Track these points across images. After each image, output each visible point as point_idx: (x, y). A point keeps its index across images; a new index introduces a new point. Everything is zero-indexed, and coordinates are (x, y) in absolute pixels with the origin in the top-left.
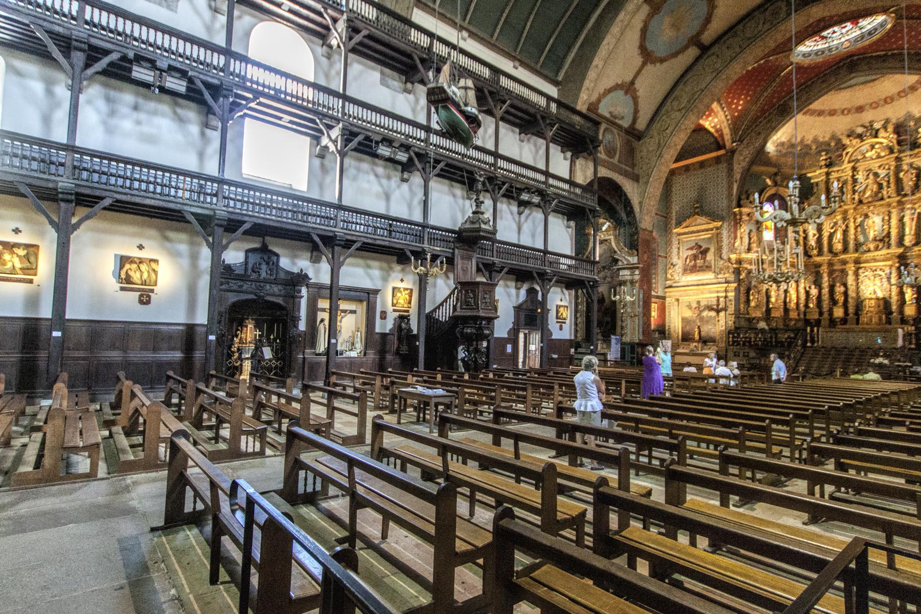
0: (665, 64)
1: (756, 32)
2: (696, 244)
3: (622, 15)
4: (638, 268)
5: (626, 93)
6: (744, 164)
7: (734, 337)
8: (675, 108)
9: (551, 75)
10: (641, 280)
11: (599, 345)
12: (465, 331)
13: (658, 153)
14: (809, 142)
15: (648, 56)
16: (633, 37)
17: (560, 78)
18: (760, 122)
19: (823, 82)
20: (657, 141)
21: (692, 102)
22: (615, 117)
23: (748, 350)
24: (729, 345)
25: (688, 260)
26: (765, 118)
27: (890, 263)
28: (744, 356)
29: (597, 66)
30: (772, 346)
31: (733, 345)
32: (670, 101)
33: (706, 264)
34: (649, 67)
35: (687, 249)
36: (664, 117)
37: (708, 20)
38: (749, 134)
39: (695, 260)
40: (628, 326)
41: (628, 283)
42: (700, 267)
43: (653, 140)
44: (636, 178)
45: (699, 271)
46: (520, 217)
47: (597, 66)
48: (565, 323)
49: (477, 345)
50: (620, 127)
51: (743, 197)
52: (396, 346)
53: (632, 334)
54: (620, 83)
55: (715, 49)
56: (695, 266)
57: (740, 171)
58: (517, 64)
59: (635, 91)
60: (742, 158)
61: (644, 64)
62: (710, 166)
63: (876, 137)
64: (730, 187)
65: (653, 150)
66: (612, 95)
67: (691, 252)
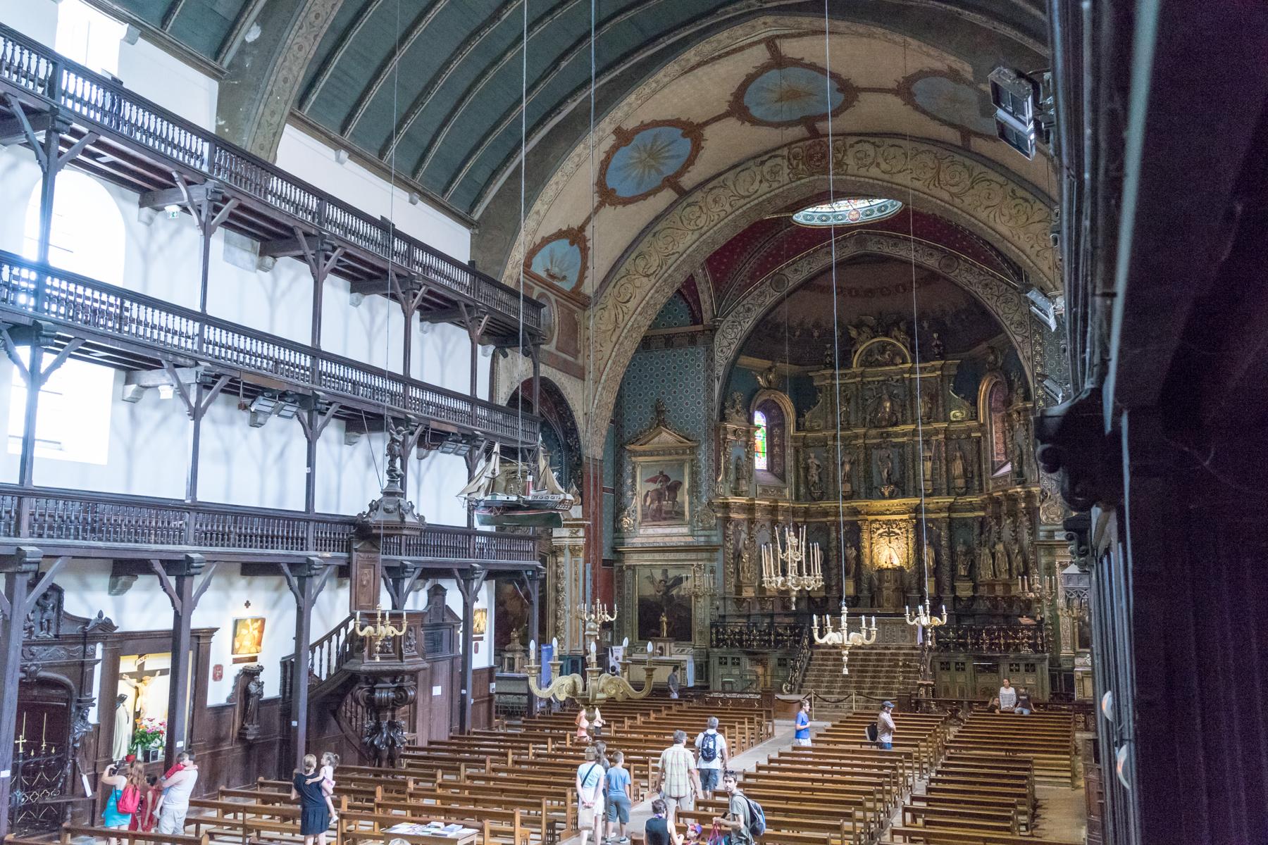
0: (632, 208)
1: (751, 190)
2: (661, 473)
3: (580, 149)
4: (583, 526)
5: (572, 244)
6: (730, 353)
7: (717, 632)
8: (641, 270)
9: (462, 212)
10: (588, 545)
11: (517, 660)
12: (377, 695)
13: (614, 339)
14: (810, 326)
15: (606, 195)
16: (590, 172)
17: (477, 216)
18: (750, 293)
20: (613, 316)
21: (665, 268)
22: (552, 277)
24: (712, 647)
25: (649, 500)
26: (756, 289)
27: (905, 517)
28: (733, 664)
29: (538, 213)
31: (717, 646)
32: (633, 256)
33: (676, 509)
34: (608, 211)
35: (648, 481)
36: (622, 281)
37: (690, 161)
39: (659, 502)
40: (568, 626)
41: (567, 552)
42: (667, 513)
43: (606, 314)
44: (580, 374)
45: (665, 519)
46: (420, 463)
47: (538, 213)
48: (481, 639)
49: (393, 717)
50: (559, 291)
51: (727, 404)
52: (237, 726)
53: (572, 640)
54: (564, 228)
55: (698, 196)
56: (659, 510)
57: (724, 362)
58: (416, 196)
59: (585, 240)
61: (601, 204)
62: (681, 346)
63: (886, 335)
64: (710, 388)
65: (604, 332)
66: (553, 244)
67: (652, 487)
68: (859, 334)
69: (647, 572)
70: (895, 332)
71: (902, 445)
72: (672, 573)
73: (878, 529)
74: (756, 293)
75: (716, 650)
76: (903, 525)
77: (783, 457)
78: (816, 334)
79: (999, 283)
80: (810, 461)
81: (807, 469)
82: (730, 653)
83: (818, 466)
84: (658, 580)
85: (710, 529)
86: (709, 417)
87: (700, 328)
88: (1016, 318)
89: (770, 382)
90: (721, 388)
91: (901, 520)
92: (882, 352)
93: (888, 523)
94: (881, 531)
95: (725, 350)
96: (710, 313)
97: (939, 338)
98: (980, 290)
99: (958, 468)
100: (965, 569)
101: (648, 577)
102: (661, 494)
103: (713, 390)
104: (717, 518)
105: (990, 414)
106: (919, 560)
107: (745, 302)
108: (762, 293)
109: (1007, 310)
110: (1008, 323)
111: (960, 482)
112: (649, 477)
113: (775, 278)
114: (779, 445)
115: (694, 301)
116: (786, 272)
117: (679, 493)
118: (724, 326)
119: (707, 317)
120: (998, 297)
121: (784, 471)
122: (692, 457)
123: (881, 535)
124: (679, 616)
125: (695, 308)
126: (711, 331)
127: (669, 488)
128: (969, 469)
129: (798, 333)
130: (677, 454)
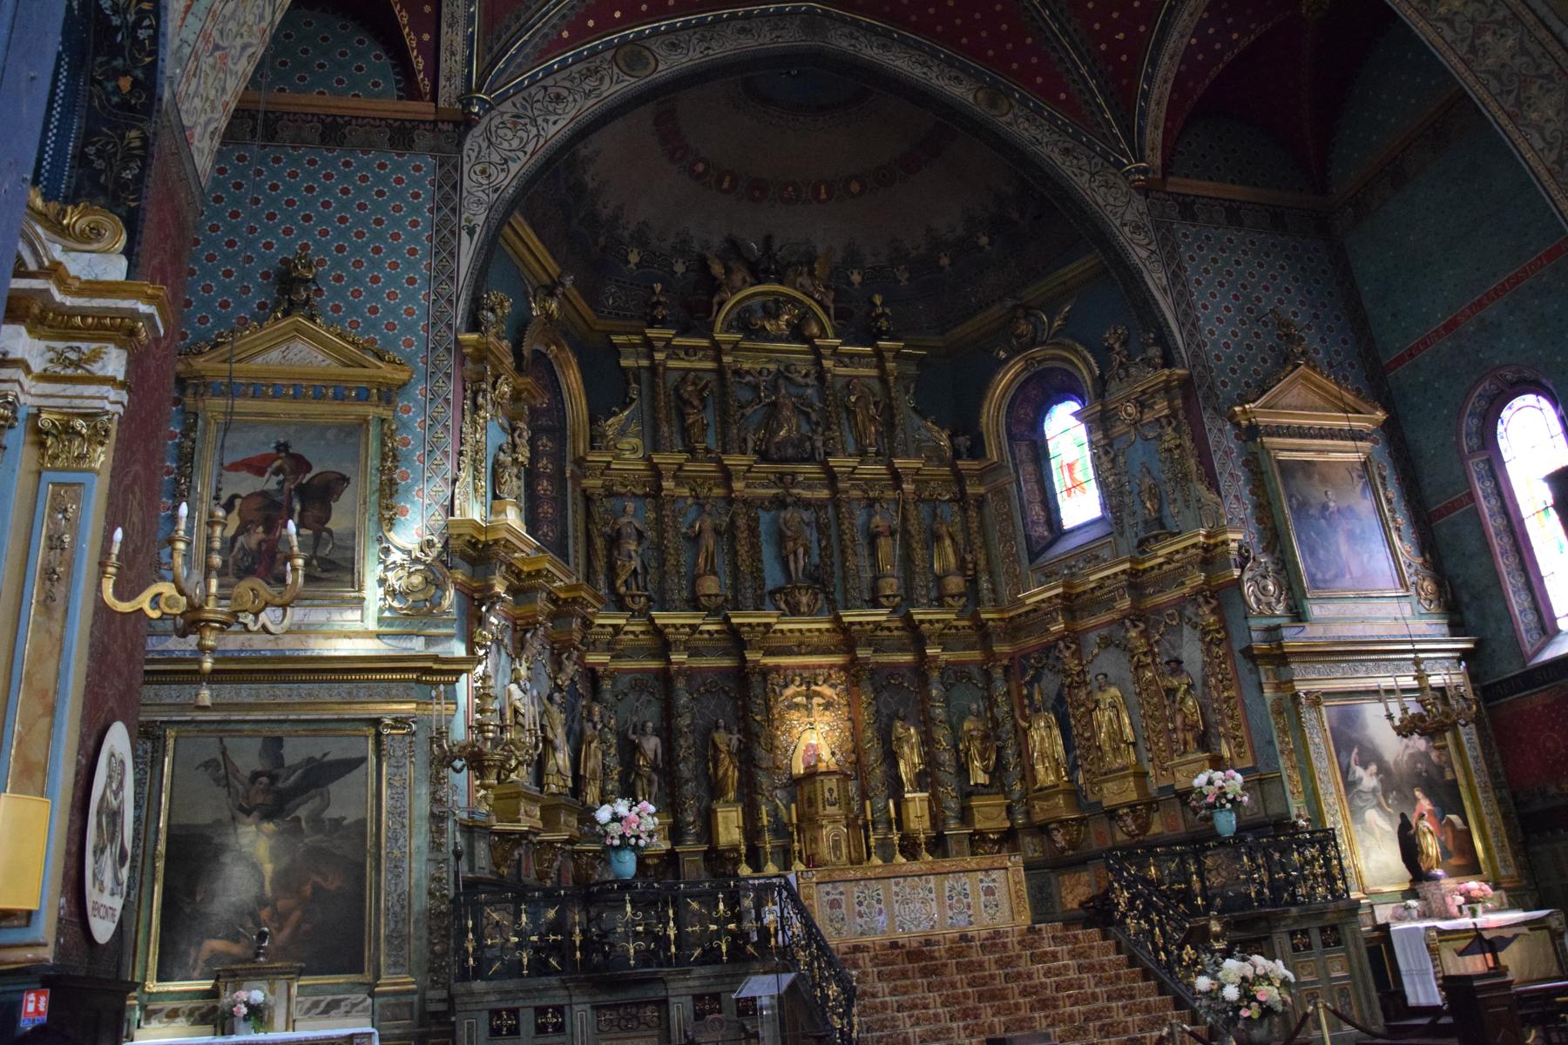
2: (282, 447)
6: (501, 179)
18: (564, 66)
19: (743, 30)
23: (559, 998)
26: (578, 59)
28: (541, 1029)
30: (668, 962)
31: (478, 973)
38: (519, 88)
39: (269, 529)
60: (496, 158)
62: (367, 146)
63: (781, 283)
64: (445, 247)
67: (246, 484)
68: (728, 271)
69: (209, 748)
71: (819, 505)
72: (296, 751)
74: (575, 68)
75: (479, 985)
77: (560, 502)
78: (634, 258)
79: (1087, 151)
80: (624, 520)
81: (614, 540)
84: (246, 772)
86: (438, 320)
87: (422, 109)
88: (1128, 217)
89: (549, 316)
90: (477, 253)
91: (831, 666)
92: (772, 313)
95: (492, 170)
96: (458, 82)
97: (882, 304)
98: (1058, 158)
99: (946, 557)
100: (985, 770)
101: (206, 765)
102: (276, 506)
103: (454, 255)
105: (1011, 446)
107: (549, 81)
108: (594, 72)
109: (1111, 200)
110: (1118, 223)
112: (239, 457)
113: (627, 48)
114: (550, 477)
115: (420, 42)
116: (654, 45)
117: (337, 508)
119: (449, 91)
120: (1092, 175)
121: (564, 535)
122: (387, 413)
124: (317, 889)
125: (419, 63)
126: (456, 124)
127: (303, 492)
128: (969, 557)
130: (340, 397)
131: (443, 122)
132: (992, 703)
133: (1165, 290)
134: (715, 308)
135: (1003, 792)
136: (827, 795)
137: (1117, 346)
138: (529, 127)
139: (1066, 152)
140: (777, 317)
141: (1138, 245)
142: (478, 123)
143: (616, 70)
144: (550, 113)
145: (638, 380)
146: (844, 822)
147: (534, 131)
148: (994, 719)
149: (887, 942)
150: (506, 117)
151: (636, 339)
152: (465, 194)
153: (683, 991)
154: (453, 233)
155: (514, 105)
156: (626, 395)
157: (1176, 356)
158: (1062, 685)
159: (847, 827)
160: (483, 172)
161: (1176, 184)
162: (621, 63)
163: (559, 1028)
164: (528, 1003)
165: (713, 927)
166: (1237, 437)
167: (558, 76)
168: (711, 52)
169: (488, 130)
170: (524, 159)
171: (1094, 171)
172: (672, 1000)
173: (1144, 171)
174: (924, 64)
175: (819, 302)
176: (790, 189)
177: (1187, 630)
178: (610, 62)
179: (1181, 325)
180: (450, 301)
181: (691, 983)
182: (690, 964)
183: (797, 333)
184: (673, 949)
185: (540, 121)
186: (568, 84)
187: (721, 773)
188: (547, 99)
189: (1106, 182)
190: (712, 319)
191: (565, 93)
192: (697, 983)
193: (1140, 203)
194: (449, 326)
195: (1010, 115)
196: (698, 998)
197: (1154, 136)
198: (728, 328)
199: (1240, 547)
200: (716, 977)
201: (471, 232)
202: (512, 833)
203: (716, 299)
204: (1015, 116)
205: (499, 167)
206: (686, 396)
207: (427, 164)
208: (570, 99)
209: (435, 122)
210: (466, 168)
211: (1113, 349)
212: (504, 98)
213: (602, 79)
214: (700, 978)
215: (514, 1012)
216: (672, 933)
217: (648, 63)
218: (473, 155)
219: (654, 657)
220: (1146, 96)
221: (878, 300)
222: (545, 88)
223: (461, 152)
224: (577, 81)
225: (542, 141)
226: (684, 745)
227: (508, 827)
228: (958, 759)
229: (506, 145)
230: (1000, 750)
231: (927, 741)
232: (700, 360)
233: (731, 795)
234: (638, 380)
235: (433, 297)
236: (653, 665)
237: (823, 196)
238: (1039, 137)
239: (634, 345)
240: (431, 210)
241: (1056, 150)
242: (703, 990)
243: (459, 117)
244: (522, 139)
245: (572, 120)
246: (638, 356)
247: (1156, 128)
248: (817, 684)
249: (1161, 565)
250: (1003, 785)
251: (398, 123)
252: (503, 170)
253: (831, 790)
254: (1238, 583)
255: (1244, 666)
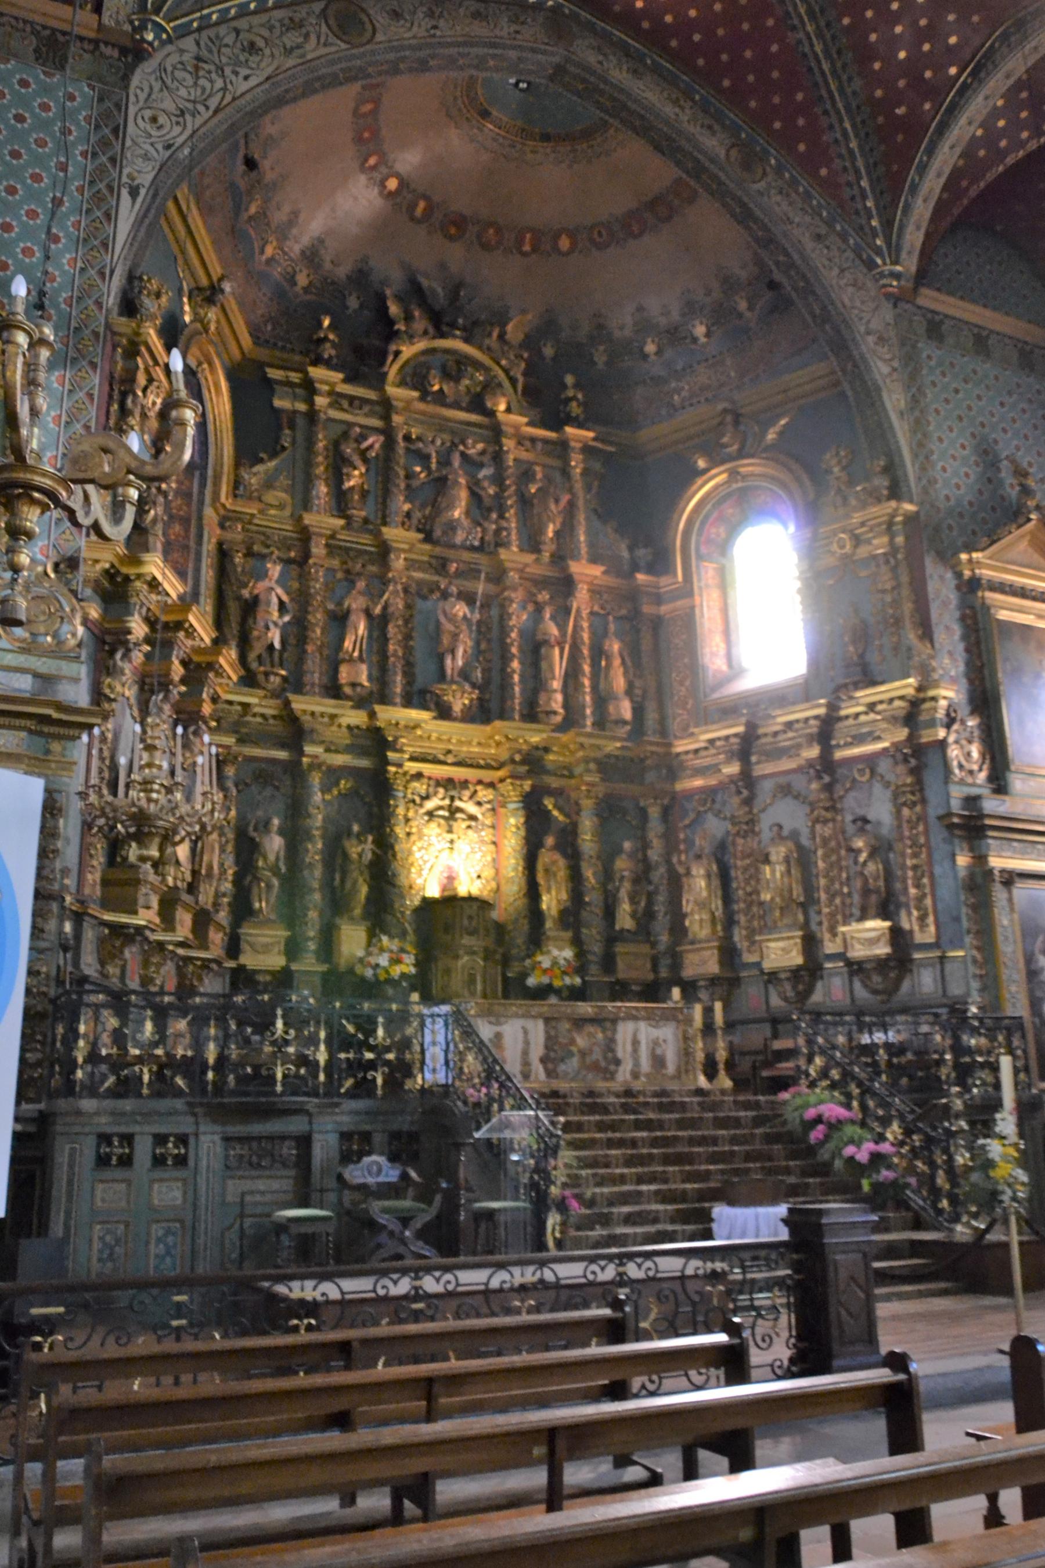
23: (185, 1125)
28: (159, 1161)
60: (168, 105)
63: (467, 340)
68: (408, 318)
70: (493, 341)
73: (427, 797)
75: (88, 1104)
76: (484, 794)
81: (251, 607)
82: (147, 1116)
83: (282, 606)
85: (58, 652)
88: (873, 325)
91: (480, 782)
93: (448, 783)
94: (430, 805)
95: (162, 119)
98: (809, 244)
100: (634, 915)
103: (109, 217)
104: (85, 622)
106: (533, 891)
107: (242, 24)
109: (858, 304)
110: (862, 329)
111: (626, 709)
118: (166, 57)
120: (842, 271)
123: (430, 814)
126: (124, 51)
128: (638, 683)
129: (269, 251)
131: (106, 44)
132: (645, 845)
133: (902, 413)
134: (390, 358)
135: (648, 941)
136: (466, 922)
137: (836, 470)
138: (214, 76)
139: (818, 237)
140: (457, 380)
141: (880, 358)
142: (150, 55)
143: (324, 28)
144: (238, 63)
145: (292, 426)
146: (482, 955)
147: (219, 83)
148: (645, 859)
149: (585, 1091)
150: (186, 57)
151: (295, 377)
152: (128, 143)
153: (329, 1127)
154: (110, 188)
155: (198, 44)
156: (277, 440)
157: (904, 489)
158: (728, 833)
159: (486, 959)
160: (154, 120)
161: (929, 298)
162: (332, 22)
163: (181, 1161)
164: (147, 1129)
165: (369, 1055)
166: (958, 588)
167: (256, 20)
168: (438, 33)
169: (161, 68)
170: (206, 115)
171: (845, 266)
172: (316, 1136)
173: (897, 276)
174: (676, 102)
175: (506, 371)
176: (491, 231)
177: (878, 788)
178: (318, 17)
179: (915, 456)
180: (102, 275)
181: (338, 1118)
182: (340, 1095)
183: (477, 403)
184: (322, 1077)
185: (228, 71)
186: (266, 33)
187: (348, 885)
188: (239, 45)
189: (855, 280)
190: (386, 369)
191: (261, 43)
192: (345, 1119)
193: (887, 313)
194: (99, 304)
195: (763, 184)
196: (345, 1136)
197: (914, 238)
198: (402, 383)
199: (949, 706)
200: (367, 1113)
201: (134, 192)
202: (126, 926)
203: (393, 347)
204: (769, 184)
205: (174, 119)
206: (348, 450)
207: (83, 95)
208: (267, 52)
209: (96, 42)
210: (132, 110)
211: (832, 472)
212: (184, 32)
213: (307, 36)
214: (350, 1112)
215: (128, 1139)
216: (322, 1056)
217: (364, 30)
218: (142, 96)
219: (283, 746)
220: (914, 189)
221: (569, 380)
222: (237, 32)
223: (126, 87)
224: (277, 32)
225: (228, 98)
226: (314, 849)
227: (124, 919)
228: (606, 899)
229: (183, 92)
230: (650, 897)
231: (575, 877)
232: (366, 415)
233: (358, 911)
234: (292, 426)
235: (79, 264)
236: (282, 755)
237: (527, 248)
238: (791, 215)
239: (289, 384)
240: (84, 154)
241: (807, 235)
242: (352, 1128)
243: (128, 44)
244: (204, 89)
245: (268, 79)
246: (295, 397)
247: (918, 228)
248: (461, 799)
249: (857, 715)
250: (649, 934)
251: (47, 32)
252: (178, 123)
253: (470, 918)
254: (943, 744)
255: (938, 835)
